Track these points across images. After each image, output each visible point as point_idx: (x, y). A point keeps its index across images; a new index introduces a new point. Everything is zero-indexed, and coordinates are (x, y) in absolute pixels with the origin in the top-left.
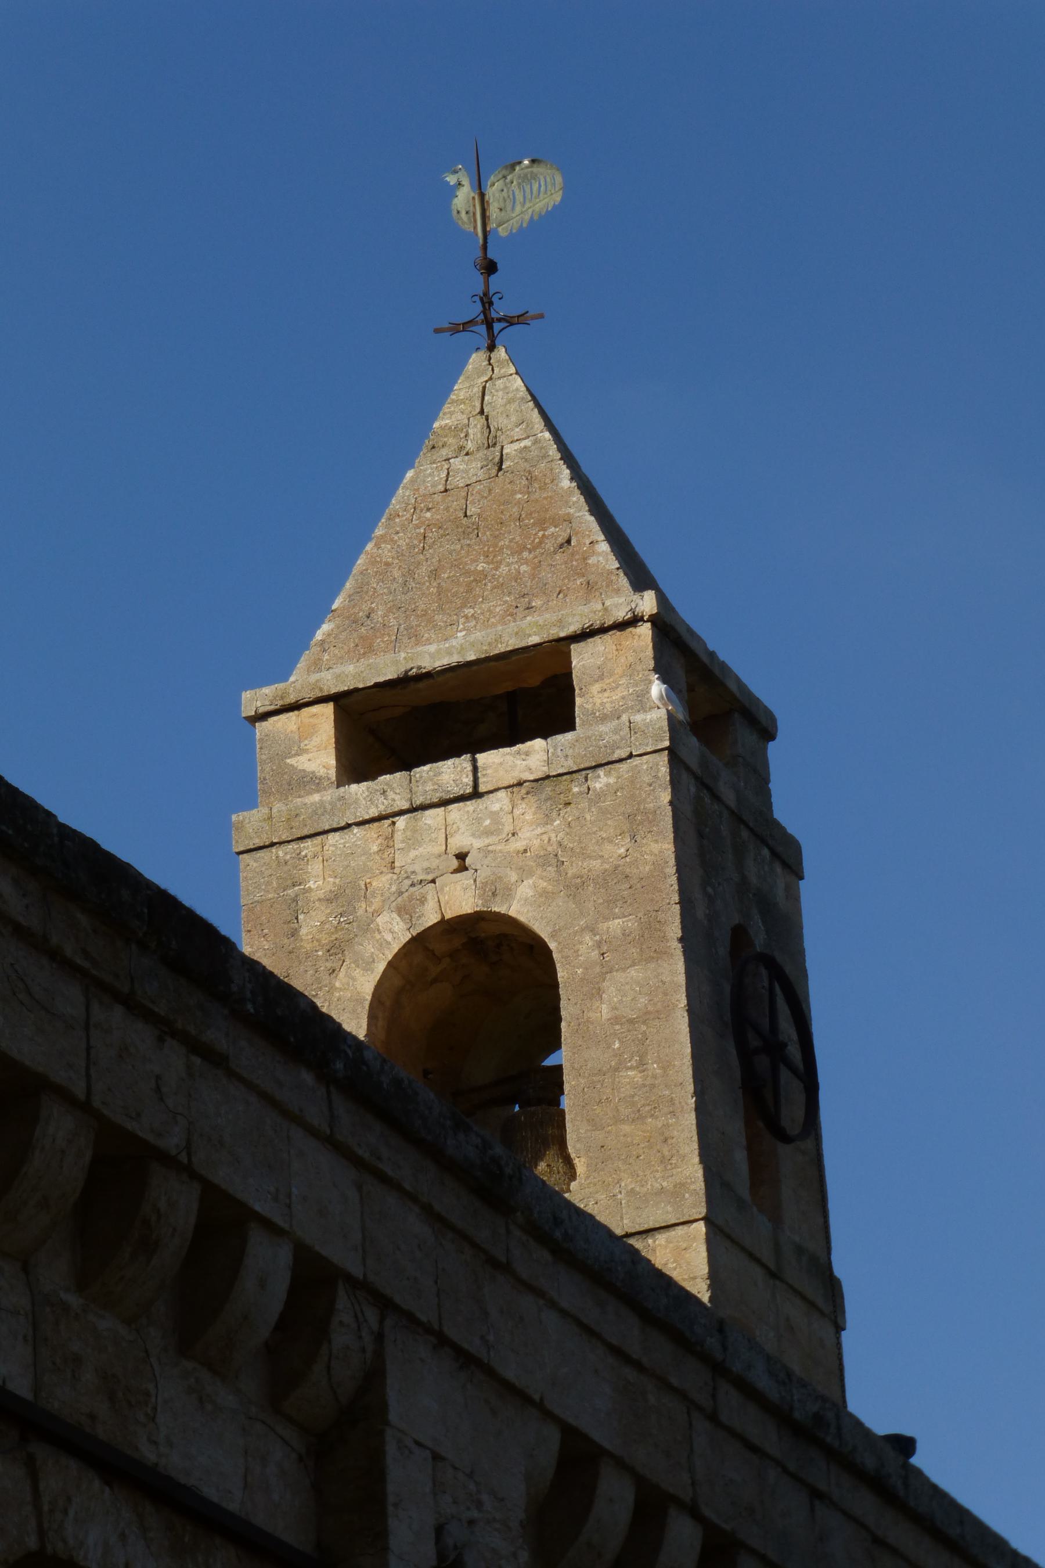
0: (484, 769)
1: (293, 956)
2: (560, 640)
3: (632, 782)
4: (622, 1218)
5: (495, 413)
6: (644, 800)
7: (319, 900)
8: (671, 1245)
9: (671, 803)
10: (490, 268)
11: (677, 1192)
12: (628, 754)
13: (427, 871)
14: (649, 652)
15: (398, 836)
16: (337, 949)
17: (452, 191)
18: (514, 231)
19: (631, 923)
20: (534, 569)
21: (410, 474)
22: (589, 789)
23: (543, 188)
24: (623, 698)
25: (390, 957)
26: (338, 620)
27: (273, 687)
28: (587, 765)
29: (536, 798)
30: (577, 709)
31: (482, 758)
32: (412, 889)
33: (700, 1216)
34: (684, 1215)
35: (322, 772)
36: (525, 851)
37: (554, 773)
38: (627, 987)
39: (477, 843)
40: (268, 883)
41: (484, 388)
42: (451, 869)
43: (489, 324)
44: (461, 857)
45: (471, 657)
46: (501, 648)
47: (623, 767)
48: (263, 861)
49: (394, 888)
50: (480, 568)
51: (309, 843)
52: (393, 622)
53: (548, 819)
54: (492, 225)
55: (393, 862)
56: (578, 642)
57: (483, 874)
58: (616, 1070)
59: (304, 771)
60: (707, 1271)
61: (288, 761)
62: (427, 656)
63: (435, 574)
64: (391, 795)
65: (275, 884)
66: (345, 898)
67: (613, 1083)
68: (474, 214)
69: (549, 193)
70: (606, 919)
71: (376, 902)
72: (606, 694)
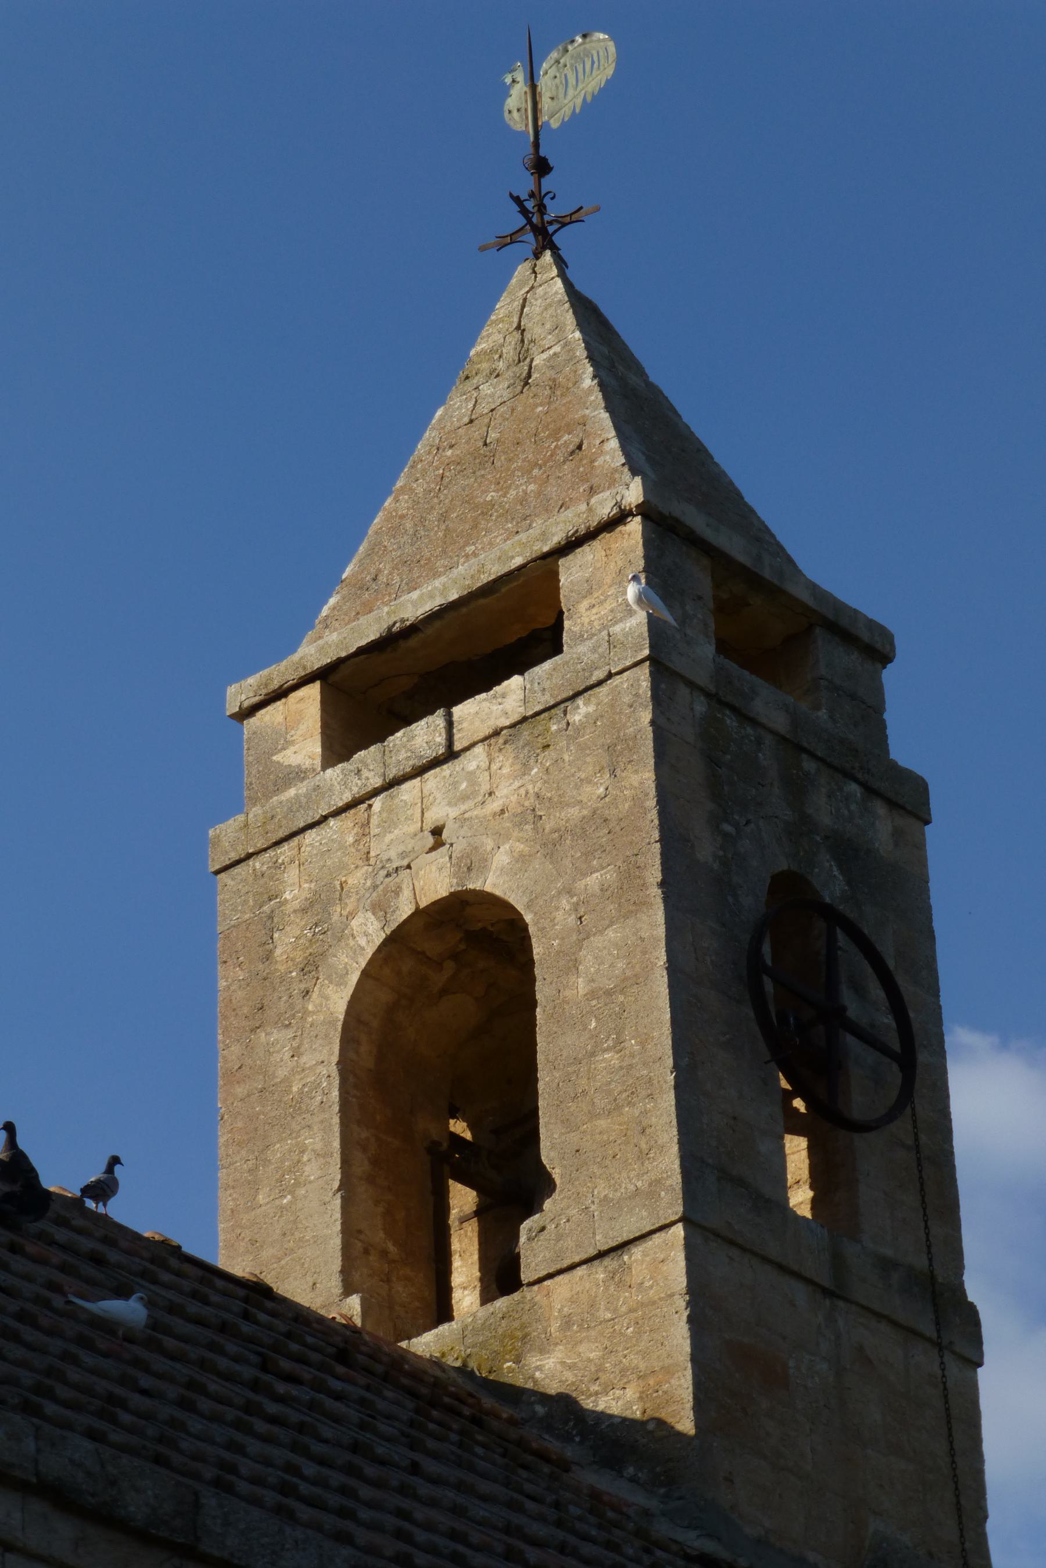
0: (460, 723)
1: (267, 983)
2: (545, 556)
3: (612, 706)
4: (594, 1234)
5: (530, 325)
7: (295, 911)
8: (648, 1259)
9: (653, 723)
10: (541, 167)
11: (651, 1193)
12: (606, 673)
13: (403, 855)
14: (640, 551)
15: (374, 821)
16: (311, 966)
17: (505, 92)
18: (566, 119)
19: (609, 875)
20: (540, 486)
21: (439, 412)
22: (568, 724)
23: (596, 65)
24: (612, 611)
25: (363, 965)
26: (345, 591)
27: (258, 675)
28: (565, 695)
29: (514, 746)
30: (564, 634)
33: (677, 1217)
36: (502, 812)
37: (531, 713)
38: (605, 952)
39: (453, 812)
40: (246, 902)
41: (525, 300)
44: (437, 832)
45: (454, 596)
46: (485, 579)
47: (603, 690)
48: (240, 877)
49: (369, 883)
50: (489, 498)
51: (286, 847)
52: (397, 579)
53: (526, 768)
54: (543, 118)
55: (368, 853)
56: (566, 555)
57: (460, 846)
58: (593, 1054)
59: (290, 766)
60: (685, 1284)
61: (274, 758)
62: (409, 605)
63: (444, 517)
64: (365, 773)
65: (251, 903)
66: (318, 906)
67: (589, 1071)
68: (526, 110)
69: (602, 68)
70: (584, 875)
71: (351, 903)
72: (594, 611)
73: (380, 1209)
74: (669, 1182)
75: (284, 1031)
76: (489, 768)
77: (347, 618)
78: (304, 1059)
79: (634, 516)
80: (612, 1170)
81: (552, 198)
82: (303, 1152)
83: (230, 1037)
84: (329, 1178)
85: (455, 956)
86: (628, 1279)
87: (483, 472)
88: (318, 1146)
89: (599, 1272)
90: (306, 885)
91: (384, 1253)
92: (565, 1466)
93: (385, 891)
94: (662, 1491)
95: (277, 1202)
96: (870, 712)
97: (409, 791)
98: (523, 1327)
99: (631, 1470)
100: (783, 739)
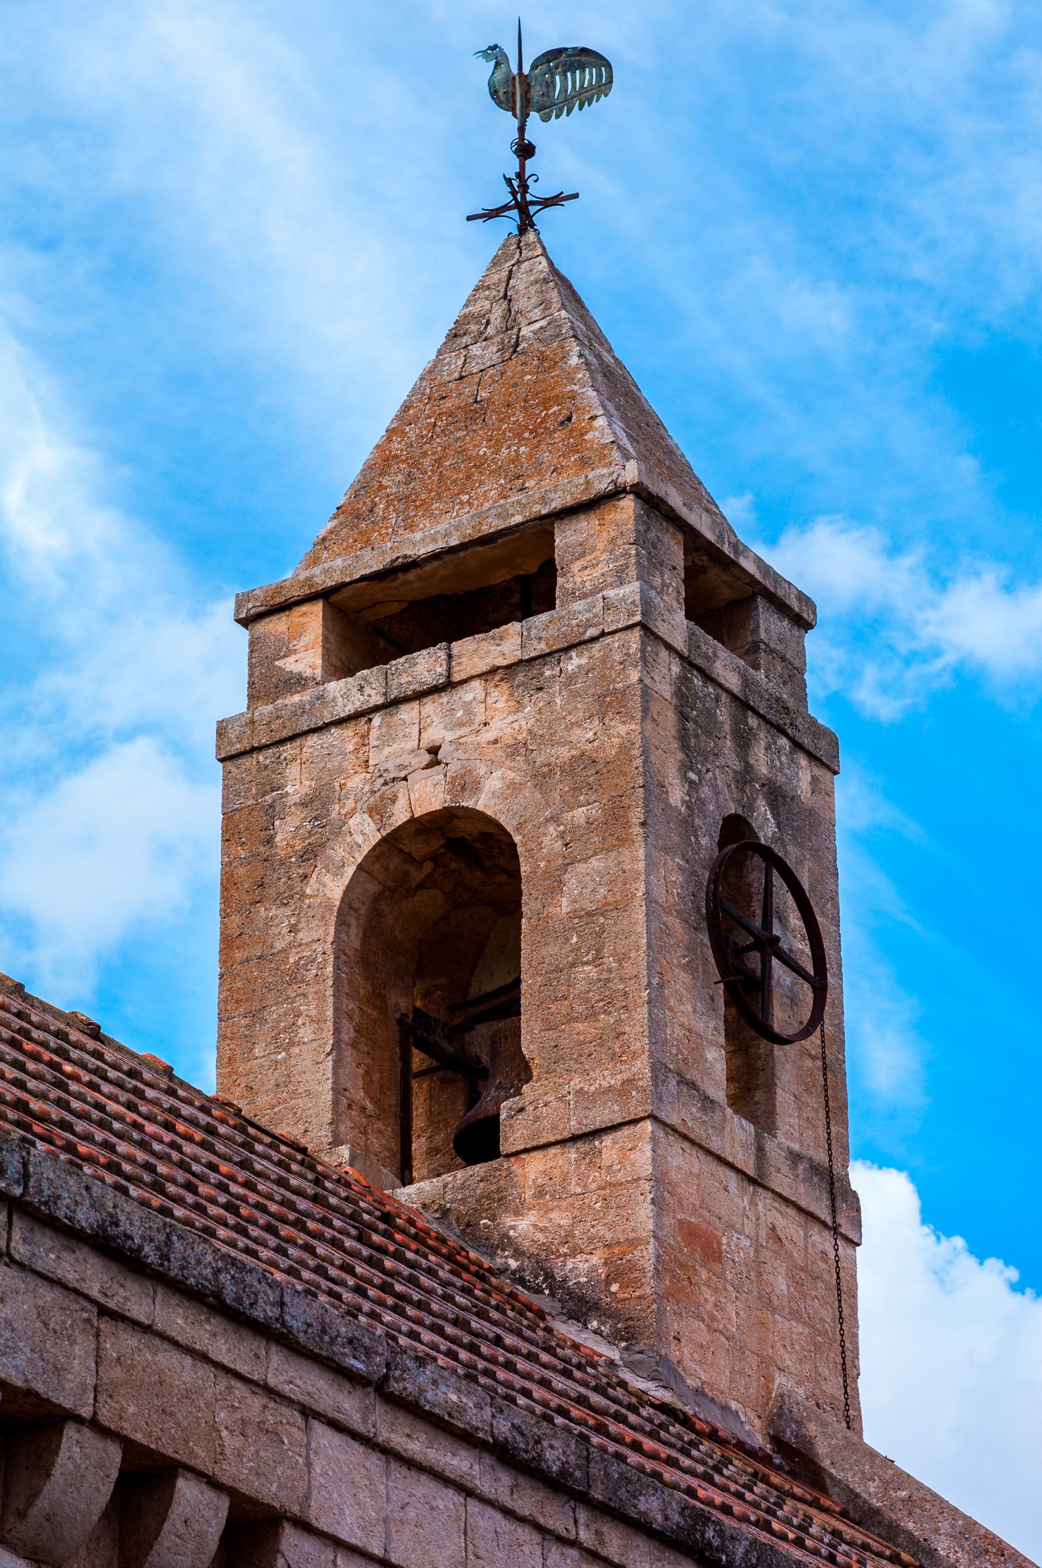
0: (459, 657)
1: (266, 864)
2: (542, 518)
6: (614, 680)
7: (295, 804)
8: (617, 1146)
13: (401, 767)
15: (374, 733)
16: (310, 854)
19: (595, 811)
20: (531, 449)
22: (561, 671)
24: (603, 575)
25: (360, 860)
31: (456, 646)
32: (385, 788)
34: (629, 1114)
35: (308, 672)
36: (496, 742)
38: (588, 878)
39: (450, 736)
40: (249, 790)
42: (423, 765)
43: (523, 207)
44: (434, 750)
45: (454, 542)
47: (597, 646)
48: (243, 767)
49: (367, 788)
53: (520, 705)
55: (367, 761)
57: (453, 768)
58: (573, 965)
61: (277, 663)
63: (439, 461)
64: (367, 690)
65: (254, 791)
66: (318, 802)
67: (569, 980)
70: (571, 809)
71: (350, 804)
72: (587, 572)
73: (361, 1071)
74: (640, 1083)
75: (282, 910)
76: (485, 701)
77: (345, 544)
78: (300, 935)
79: (628, 493)
80: (587, 1067)
81: (536, 181)
82: (298, 1016)
83: (231, 907)
84: (322, 1042)
85: (434, 858)
86: (598, 1161)
87: (474, 427)
88: (313, 1013)
89: (572, 1154)
90: (308, 783)
91: (363, 1109)
92: (541, 1315)
93: (382, 798)
94: (623, 1344)
95: (272, 1057)
96: (794, 673)
97: (408, 713)
98: (499, 1191)
99: (595, 1324)
100: (734, 697)
